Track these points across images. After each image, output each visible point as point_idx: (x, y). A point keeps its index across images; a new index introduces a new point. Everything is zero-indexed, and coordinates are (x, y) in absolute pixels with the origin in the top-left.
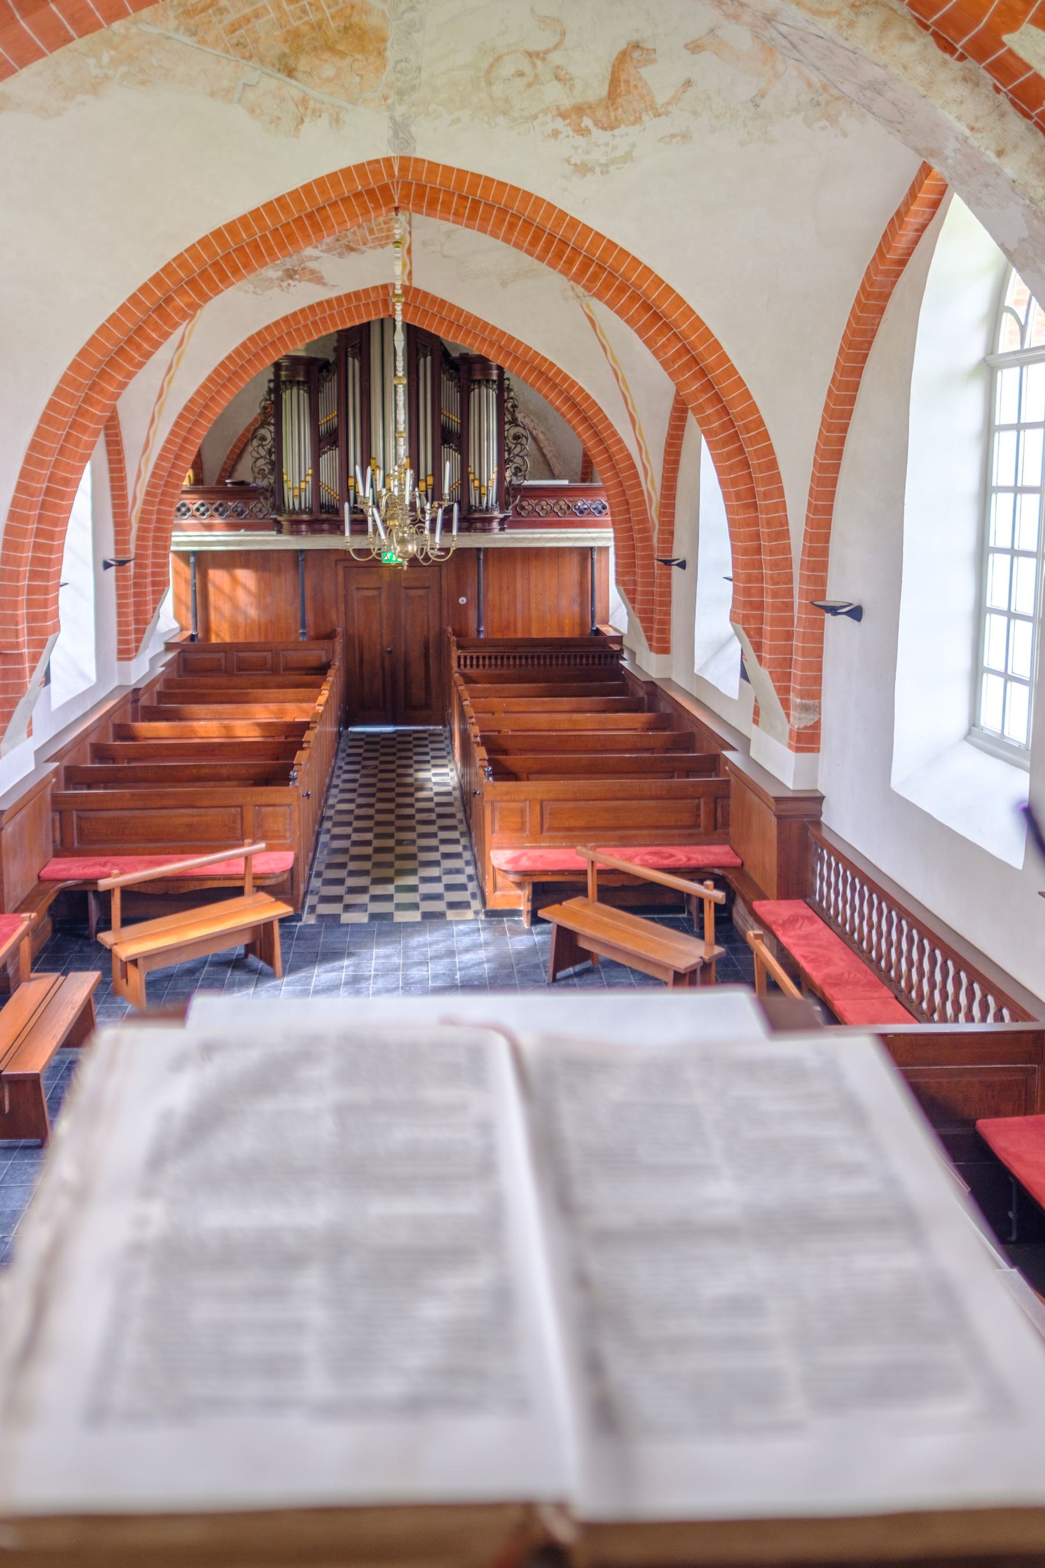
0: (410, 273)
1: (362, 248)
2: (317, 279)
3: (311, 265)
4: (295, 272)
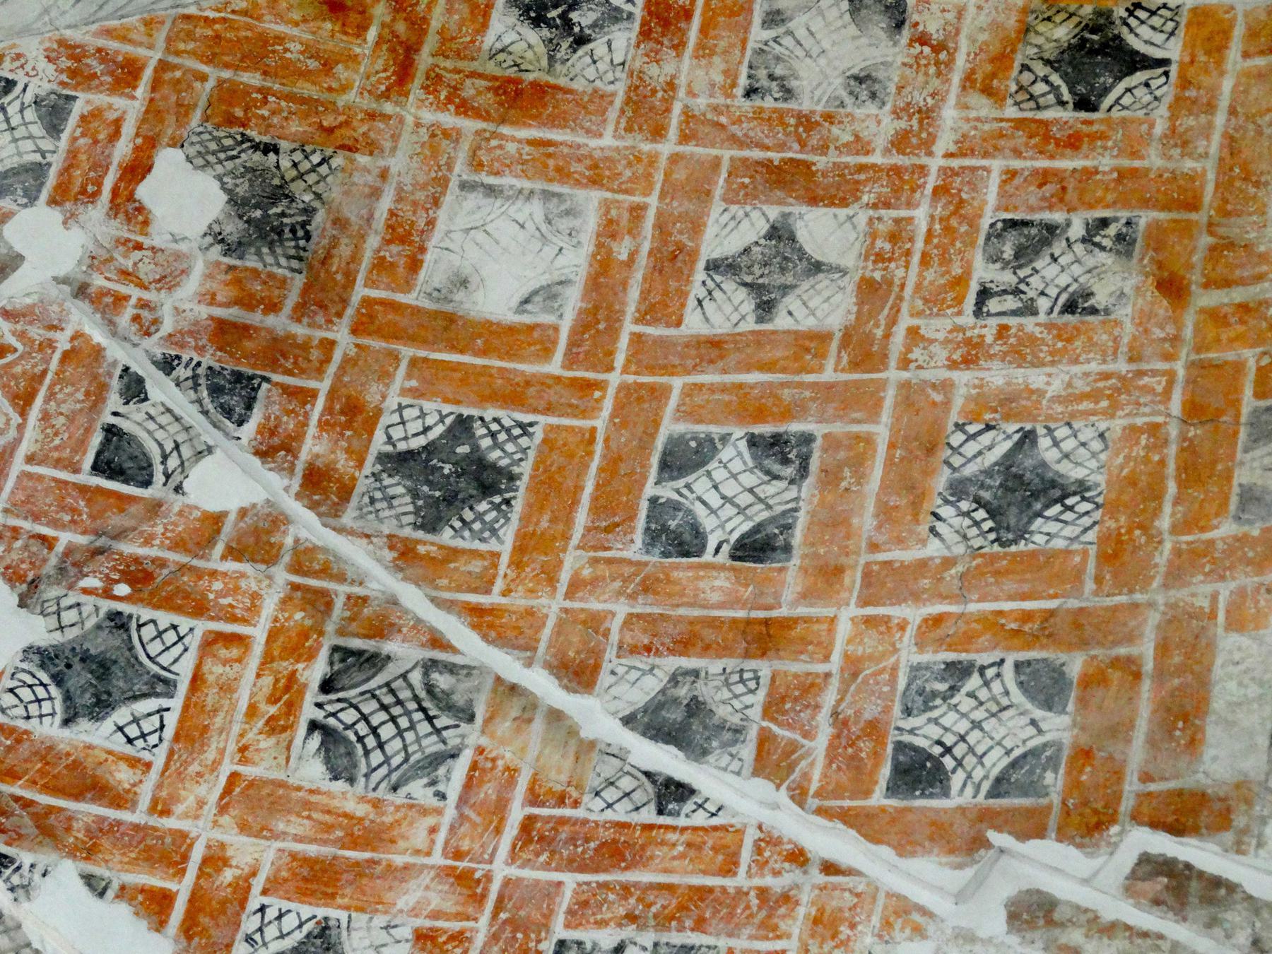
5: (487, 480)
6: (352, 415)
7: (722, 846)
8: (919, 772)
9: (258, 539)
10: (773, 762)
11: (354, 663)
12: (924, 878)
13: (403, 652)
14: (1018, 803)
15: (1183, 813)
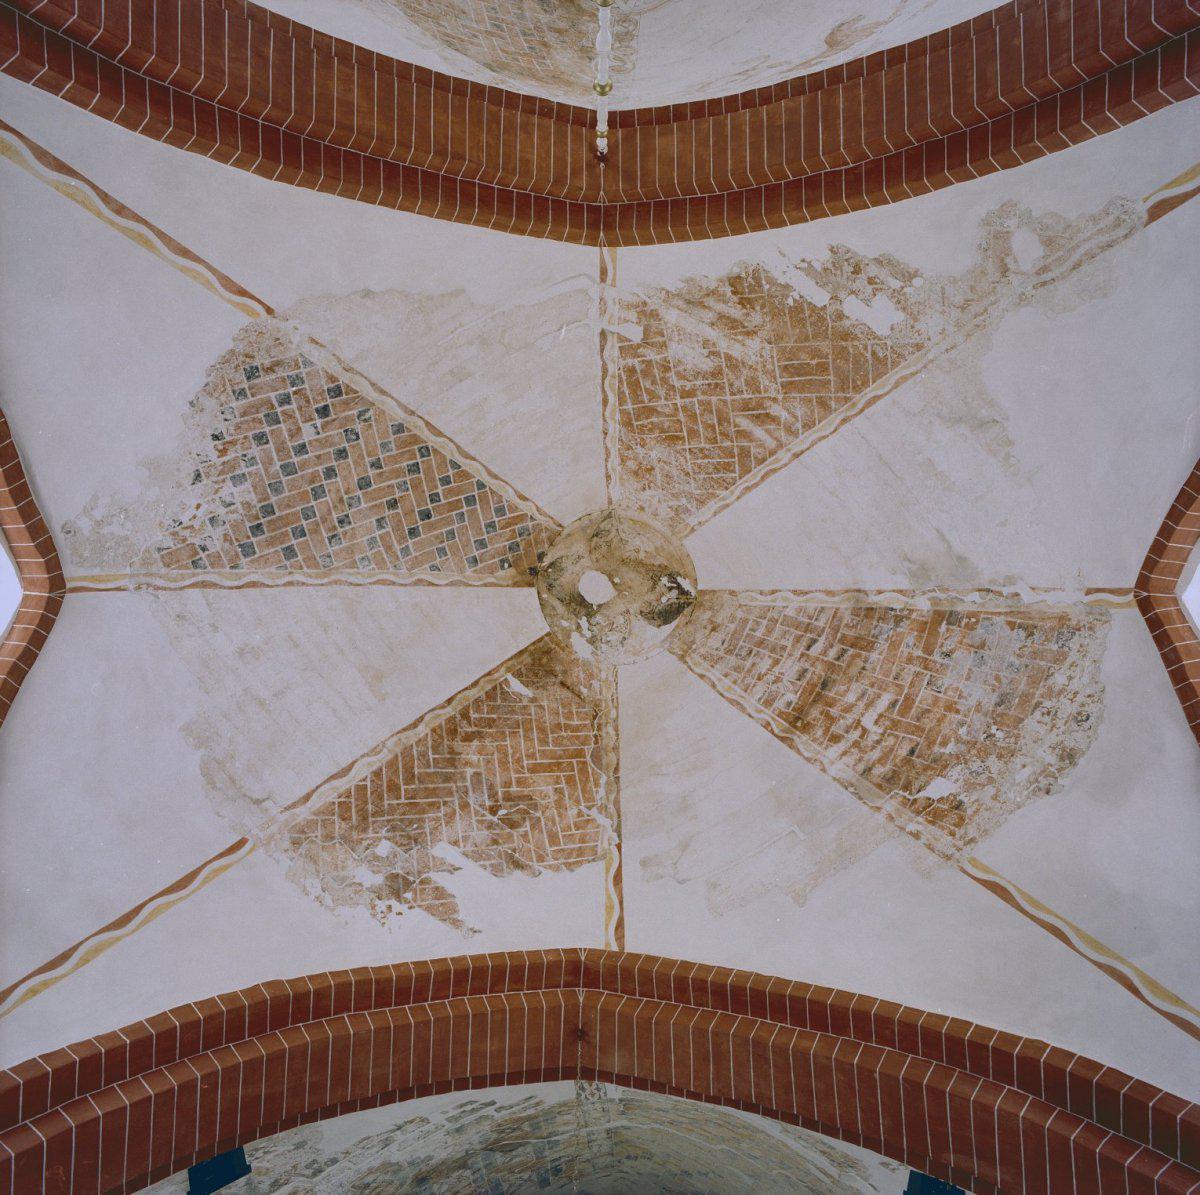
0: (620, 925)
1: (536, 865)
2: (443, 907)
3: (439, 878)
4: (408, 884)
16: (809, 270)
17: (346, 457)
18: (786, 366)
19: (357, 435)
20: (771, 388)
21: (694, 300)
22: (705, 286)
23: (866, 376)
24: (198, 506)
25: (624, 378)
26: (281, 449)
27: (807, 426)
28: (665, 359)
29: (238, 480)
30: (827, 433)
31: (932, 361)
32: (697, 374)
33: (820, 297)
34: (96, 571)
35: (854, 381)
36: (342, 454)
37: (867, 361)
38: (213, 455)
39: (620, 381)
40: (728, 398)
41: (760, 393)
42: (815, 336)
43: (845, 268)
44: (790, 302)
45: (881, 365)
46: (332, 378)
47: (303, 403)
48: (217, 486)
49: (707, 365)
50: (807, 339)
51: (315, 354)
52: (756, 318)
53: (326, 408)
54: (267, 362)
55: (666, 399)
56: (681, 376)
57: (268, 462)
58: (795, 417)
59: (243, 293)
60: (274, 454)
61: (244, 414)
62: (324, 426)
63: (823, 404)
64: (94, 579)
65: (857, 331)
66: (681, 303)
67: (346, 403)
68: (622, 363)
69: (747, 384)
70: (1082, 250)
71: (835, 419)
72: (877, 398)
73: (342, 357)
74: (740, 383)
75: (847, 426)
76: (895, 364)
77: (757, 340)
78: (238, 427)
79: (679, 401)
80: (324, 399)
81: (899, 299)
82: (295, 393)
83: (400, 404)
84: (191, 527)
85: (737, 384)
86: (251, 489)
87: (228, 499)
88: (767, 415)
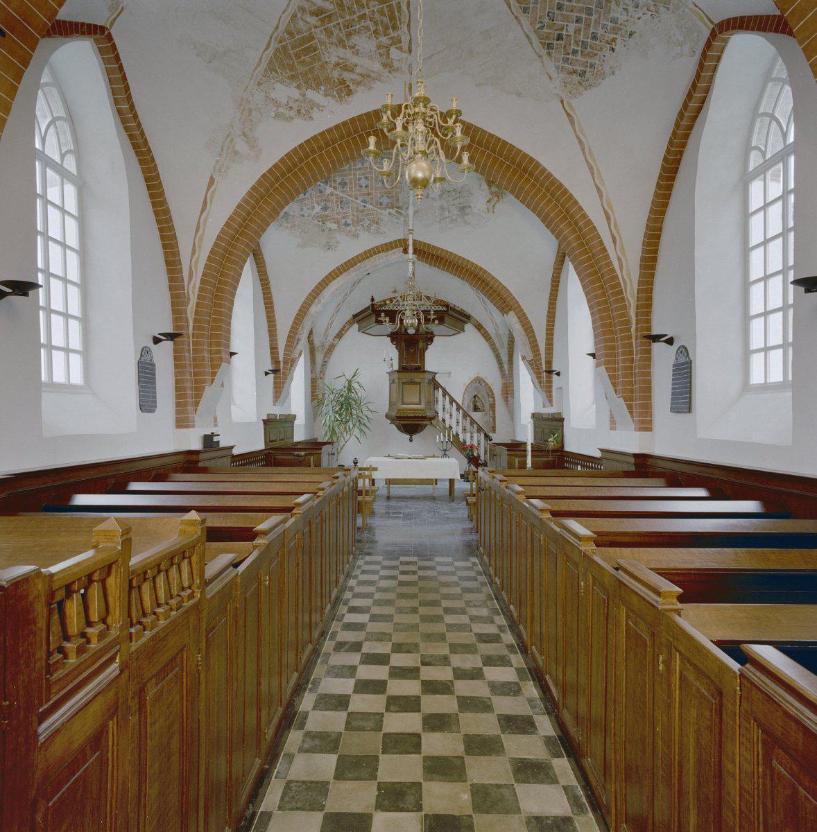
5: (346, 184)
6: (335, 181)
7: (368, 210)
8: (381, 204)
9: (332, 194)
10: (371, 204)
11: (342, 202)
12: (383, 212)
13: (344, 200)
14: (387, 207)
15: (398, 208)
16: (318, 106)
17: (558, 4)
18: (315, 51)
19: (548, 15)
20: (320, 35)
21: (367, 78)
22: (363, 87)
23: (276, 59)
24: (639, 18)
25: (398, 23)
26: (588, 25)
27: (295, 16)
28: (377, 38)
29: (614, 20)
30: (284, 16)
31: (251, 79)
32: (359, 32)
33: (310, 94)
34: (698, 21)
35: (280, 54)
36: (560, 7)
37: (279, 69)
38: (618, 41)
39: (400, 20)
40: (340, 21)
41: (324, 29)
42: (306, 73)
43: (305, 111)
44: (323, 88)
45: (271, 68)
46: (549, 54)
47: (567, 46)
48: (626, 23)
49: (355, 39)
50: (310, 70)
51: (552, 71)
52: (335, 74)
53: (558, 39)
54: (574, 76)
55: (374, 11)
56: (367, 28)
57: (597, 22)
58: (302, 20)
59: (568, 115)
60: (592, 25)
61: (596, 54)
62: (562, 29)
63: (291, 34)
64: (701, 19)
65: (288, 81)
66: (373, 75)
67: (548, 38)
68: (400, 32)
69: (332, 32)
70: (225, 155)
71: (282, 28)
72: (267, 49)
73: (541, 64)
74: (335, 32)
75: (274, 26)
76: (266, 71)
77: (333, 62)
78: (601, 49)
79: (367, 11)
80: (557, 45)
81: (277, 104)
82: (569, 54)
83: (521, 26)
84: (648, 10)
85: (337, 31)
86: (611, 11)
87: (624, 13)
88: (317, 15)
